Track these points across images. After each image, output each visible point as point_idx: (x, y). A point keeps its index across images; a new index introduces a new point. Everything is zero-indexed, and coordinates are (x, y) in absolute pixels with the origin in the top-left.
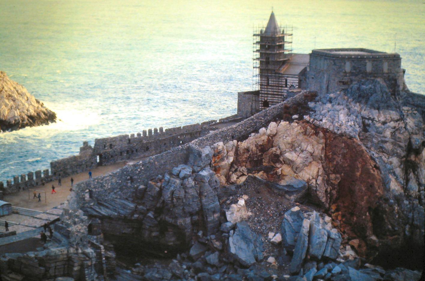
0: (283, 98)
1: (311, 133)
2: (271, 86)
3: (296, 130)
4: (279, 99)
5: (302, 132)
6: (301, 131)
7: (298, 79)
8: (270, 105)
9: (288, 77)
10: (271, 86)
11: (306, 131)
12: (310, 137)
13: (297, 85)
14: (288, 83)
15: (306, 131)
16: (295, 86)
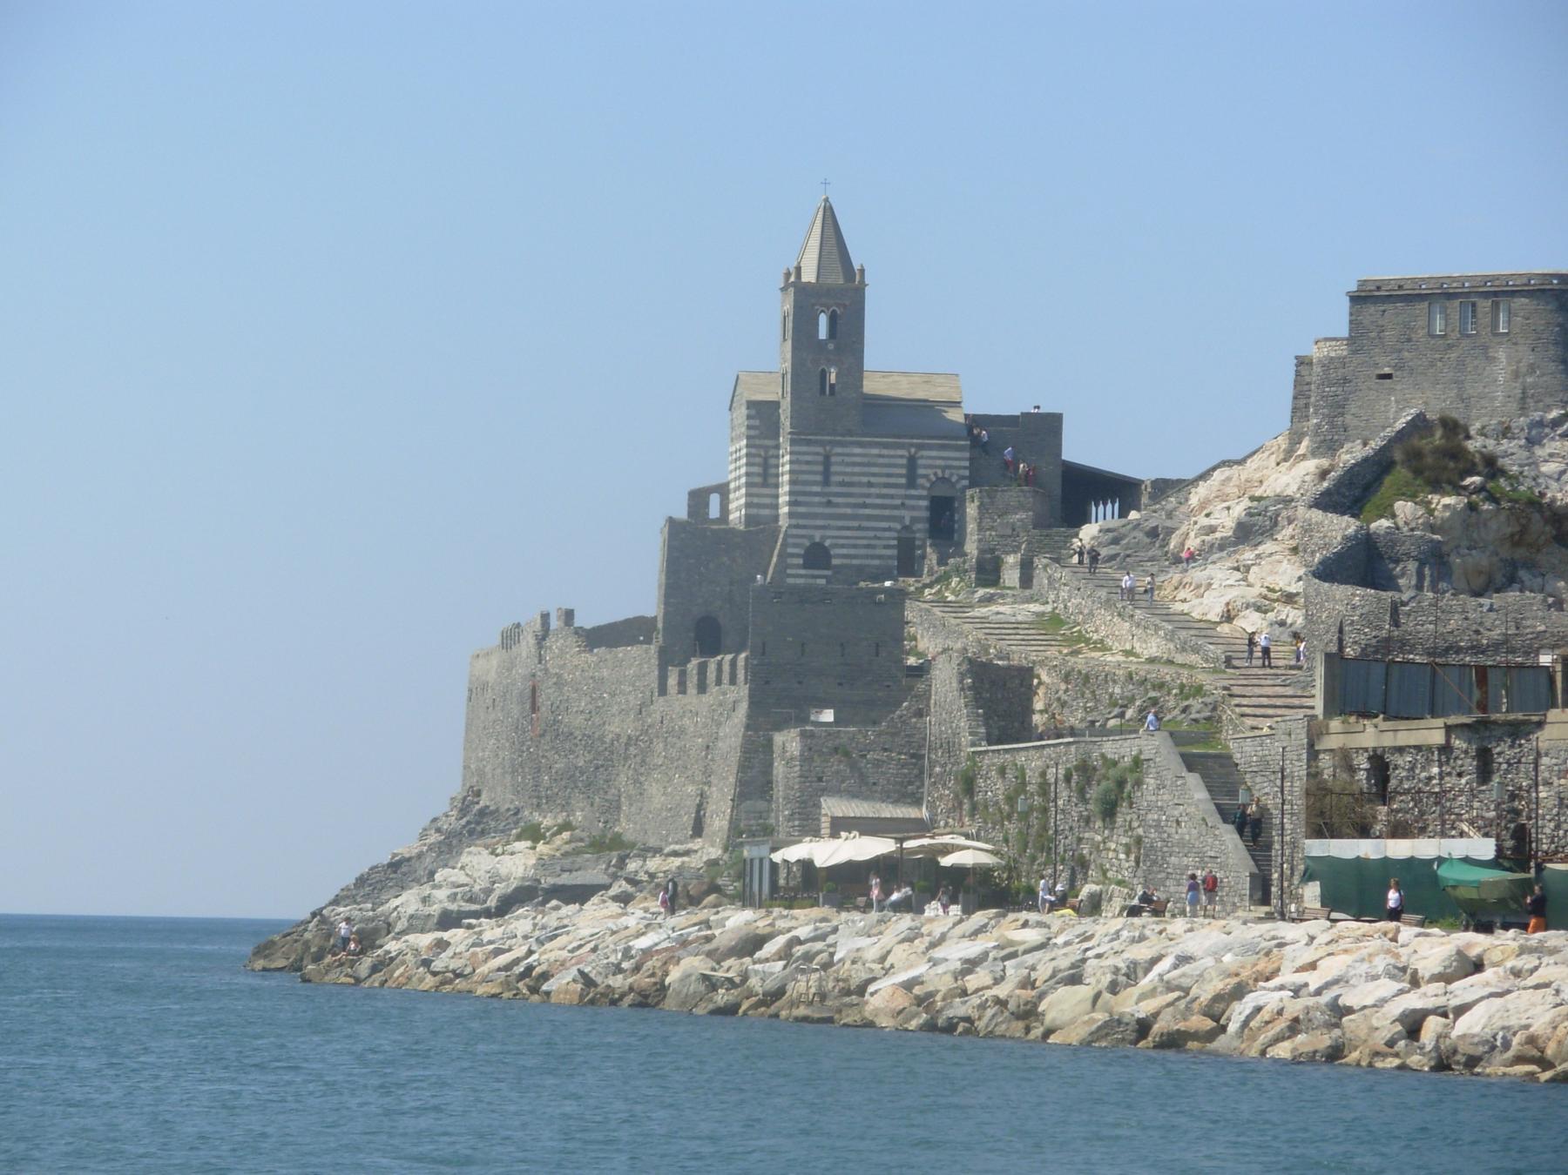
0: (898, 532)
1: (1543, 538)
2: (842, 484)
3: (1493, 525)
4: (879, 534)
5: (1512, 535)
6: (1509, 530)
7: (967, 455)
8: (835, 562)
9: (921, 447)
10: (842, 484)
11: (1524, 531)
12: (1538, 550)
13: (963, 478)
14: (921, 471)
15: (1524, 531)
16: (954, 479)
